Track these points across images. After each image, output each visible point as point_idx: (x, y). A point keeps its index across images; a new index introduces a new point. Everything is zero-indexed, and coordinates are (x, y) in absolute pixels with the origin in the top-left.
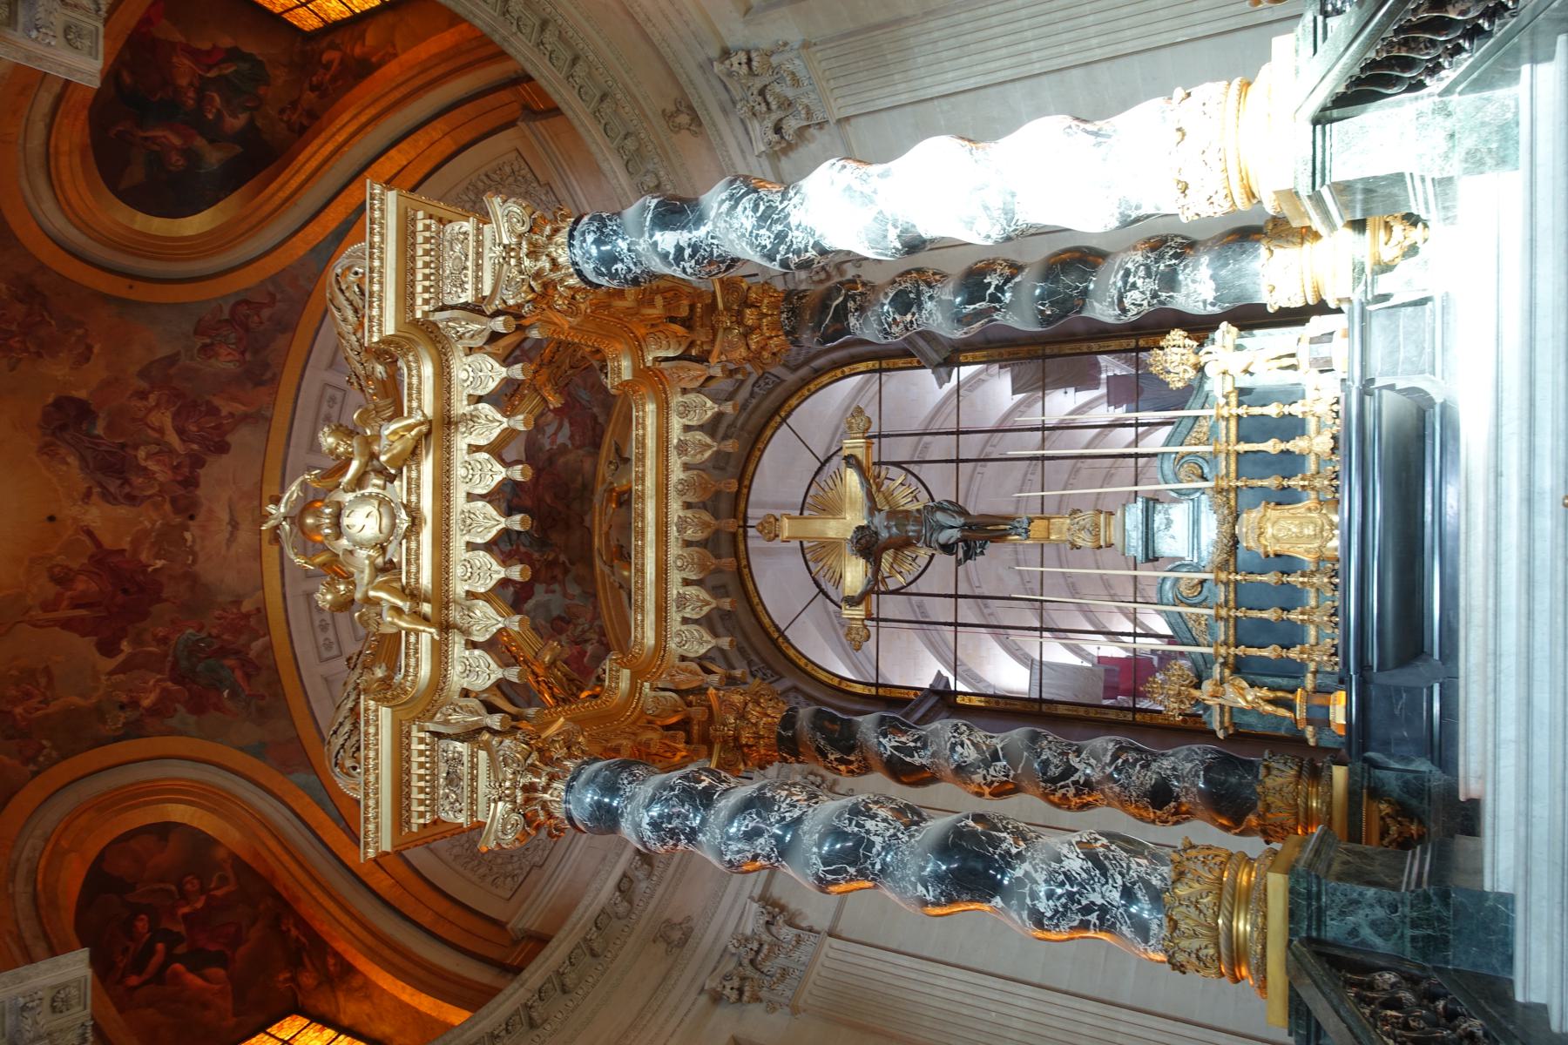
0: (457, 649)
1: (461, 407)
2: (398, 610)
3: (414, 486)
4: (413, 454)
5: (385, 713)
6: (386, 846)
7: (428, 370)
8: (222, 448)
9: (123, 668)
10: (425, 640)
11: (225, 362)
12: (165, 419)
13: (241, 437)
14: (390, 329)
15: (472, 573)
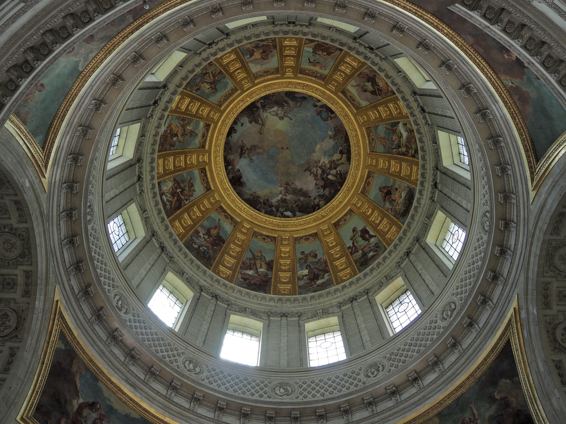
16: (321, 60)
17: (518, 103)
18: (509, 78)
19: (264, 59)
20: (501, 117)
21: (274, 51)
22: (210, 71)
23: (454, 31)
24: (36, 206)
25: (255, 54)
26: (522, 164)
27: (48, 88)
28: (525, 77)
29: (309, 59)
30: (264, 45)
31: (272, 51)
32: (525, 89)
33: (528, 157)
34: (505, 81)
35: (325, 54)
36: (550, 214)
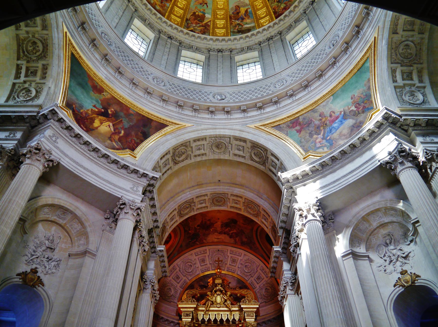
0: (203, 313)
1: (233, 313)
2: (208, 306)
3: (223, 307)
4: (227, 307)
5: (195, 306)
6: (180, 306)
7: (237, 309)
8: (231, 237)
9: (195, 228)
10: (204, 309)
11: (244, 240)
12: (235, 231)
13: (232, 241)
14: (242, 306)
15: (212, 315)
16: (199, 7)
17: (96, 84)
18: (107, 97)
19: (238, 6)
20: (100, 69)
21: (231, 13)
22: (276, 3)
23: (140, 114)
24: (386, 24)
25: (244, 12)
26: (77, 44)
27: (350, 95)
28: (100, 102)
29: (207, 6)
30: (238, 20)
31: (233, 13)
32: (97, 94)
33: (78, 53)
34: (107, 94)
35: (197, 13)
36: (53, 26)
